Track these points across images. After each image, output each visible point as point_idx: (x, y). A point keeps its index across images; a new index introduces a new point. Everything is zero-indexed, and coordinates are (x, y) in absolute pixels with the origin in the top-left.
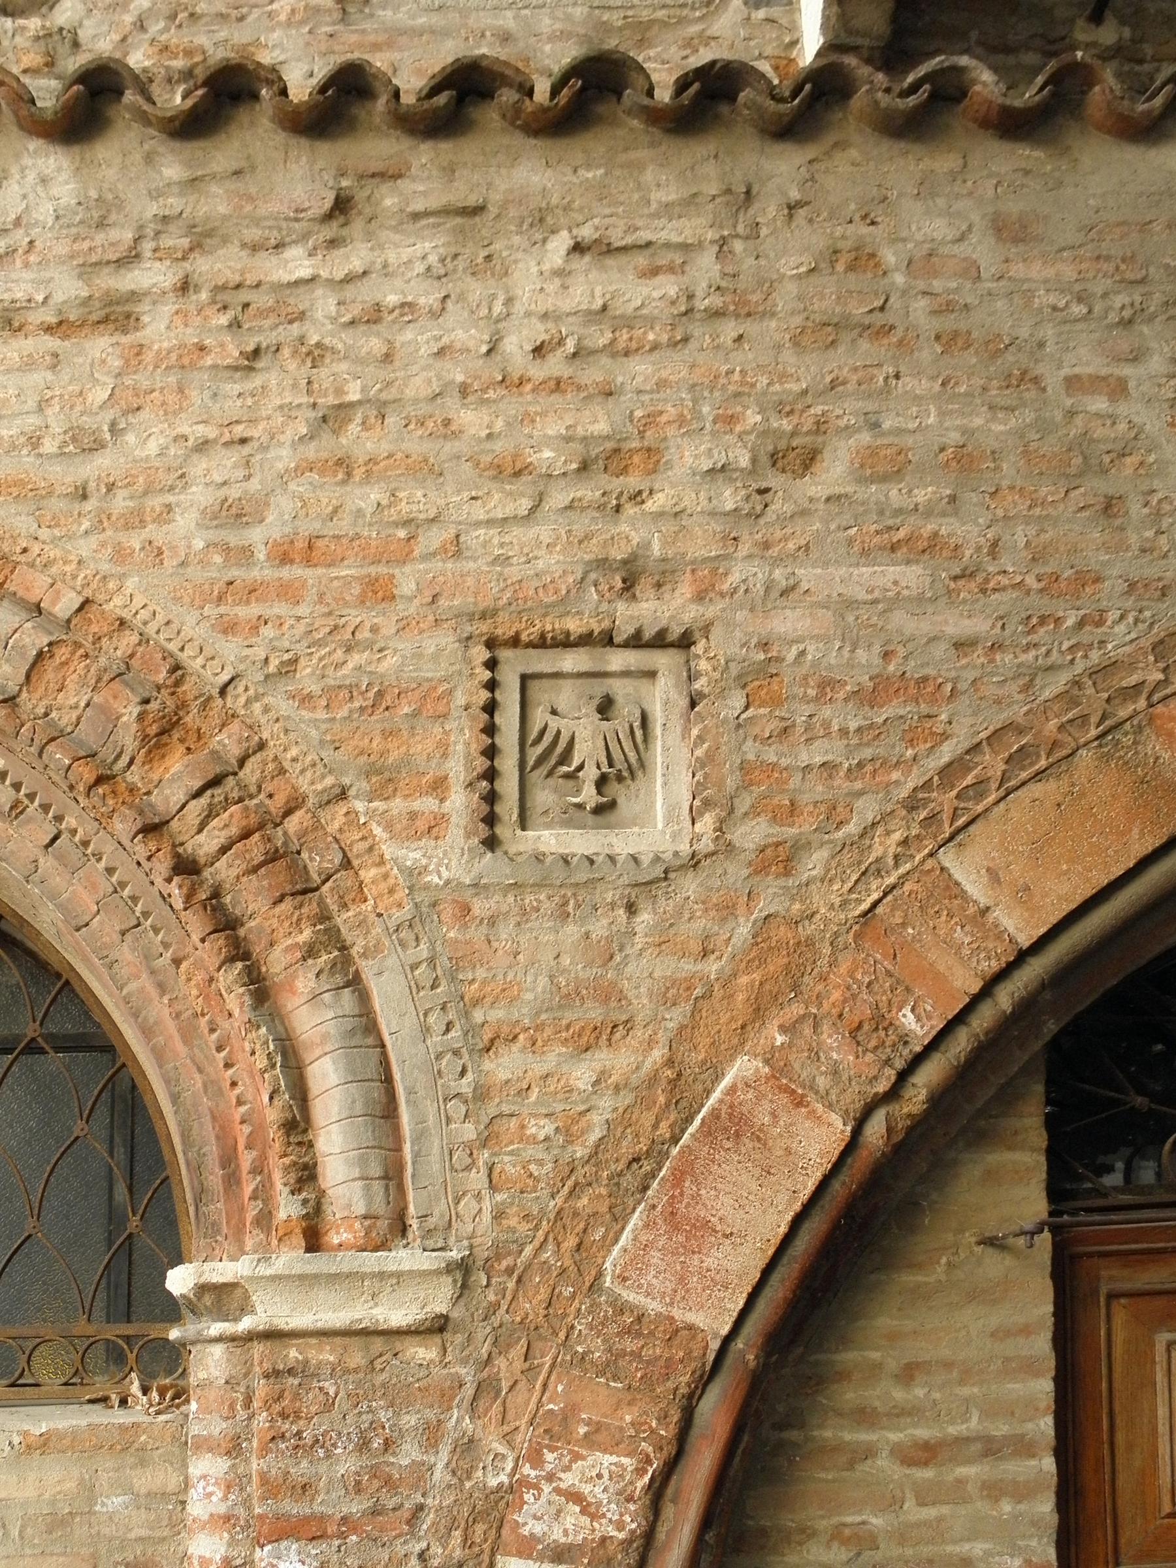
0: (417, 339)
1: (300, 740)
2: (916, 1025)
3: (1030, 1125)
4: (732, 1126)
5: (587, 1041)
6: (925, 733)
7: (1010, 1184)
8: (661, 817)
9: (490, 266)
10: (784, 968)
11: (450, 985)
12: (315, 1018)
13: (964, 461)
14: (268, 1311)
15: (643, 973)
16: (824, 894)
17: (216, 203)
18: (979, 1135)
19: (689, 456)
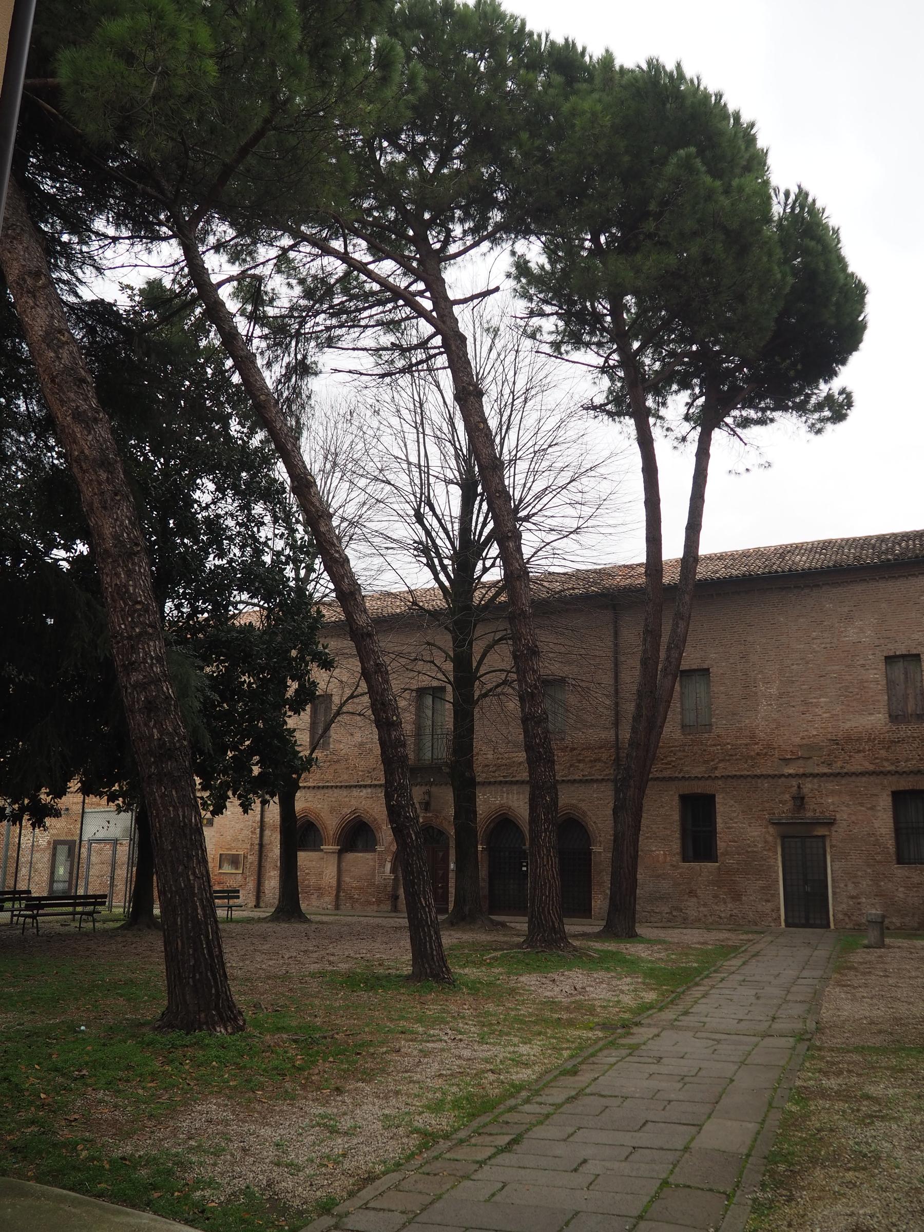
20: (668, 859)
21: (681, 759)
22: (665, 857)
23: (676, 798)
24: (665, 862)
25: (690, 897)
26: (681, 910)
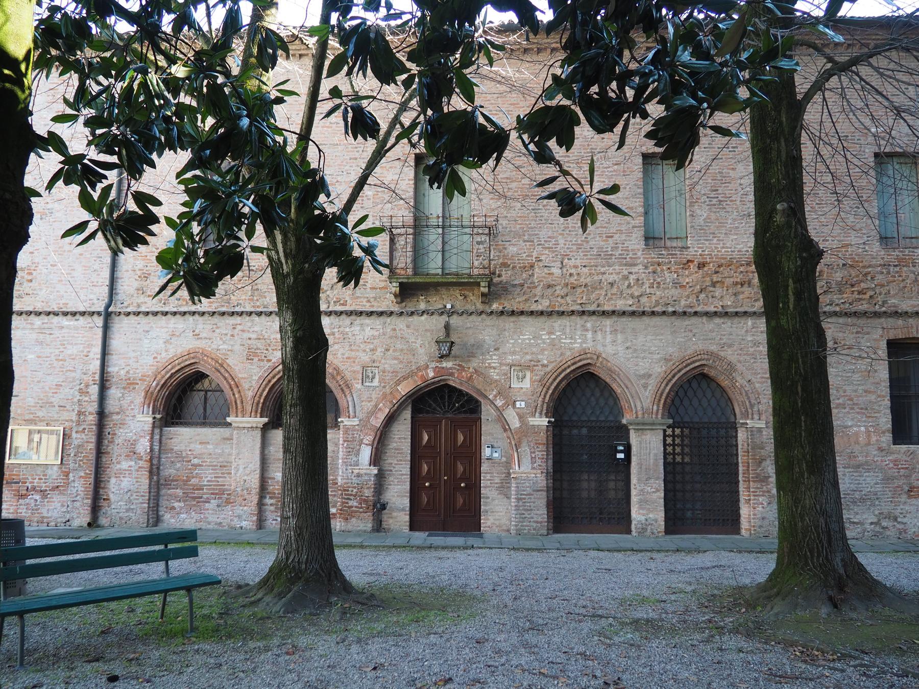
0: (358, 337)
1: (348, 375)
2: (395, 402)
3: (410, 408)
4: (380, 409)
5: (369, 402)
6: (396, 376)
7: (407, 414)
8: (376, 383)
9: (364, 330)
10: (385, 396)
11: (359, 396)
12: (350, 399)
13: (402, 350)
14: (346, 423)
15: (374, 396)
16: (388, 390)
17: (341, 323)
18: (404, 409)
19: (379, 350)
20: (874, 439)
21: (882, 286)
22: (869, 436)
23: (884, 344)
24: (869, 444)
25: (910, 497)
26: (895, 519)
